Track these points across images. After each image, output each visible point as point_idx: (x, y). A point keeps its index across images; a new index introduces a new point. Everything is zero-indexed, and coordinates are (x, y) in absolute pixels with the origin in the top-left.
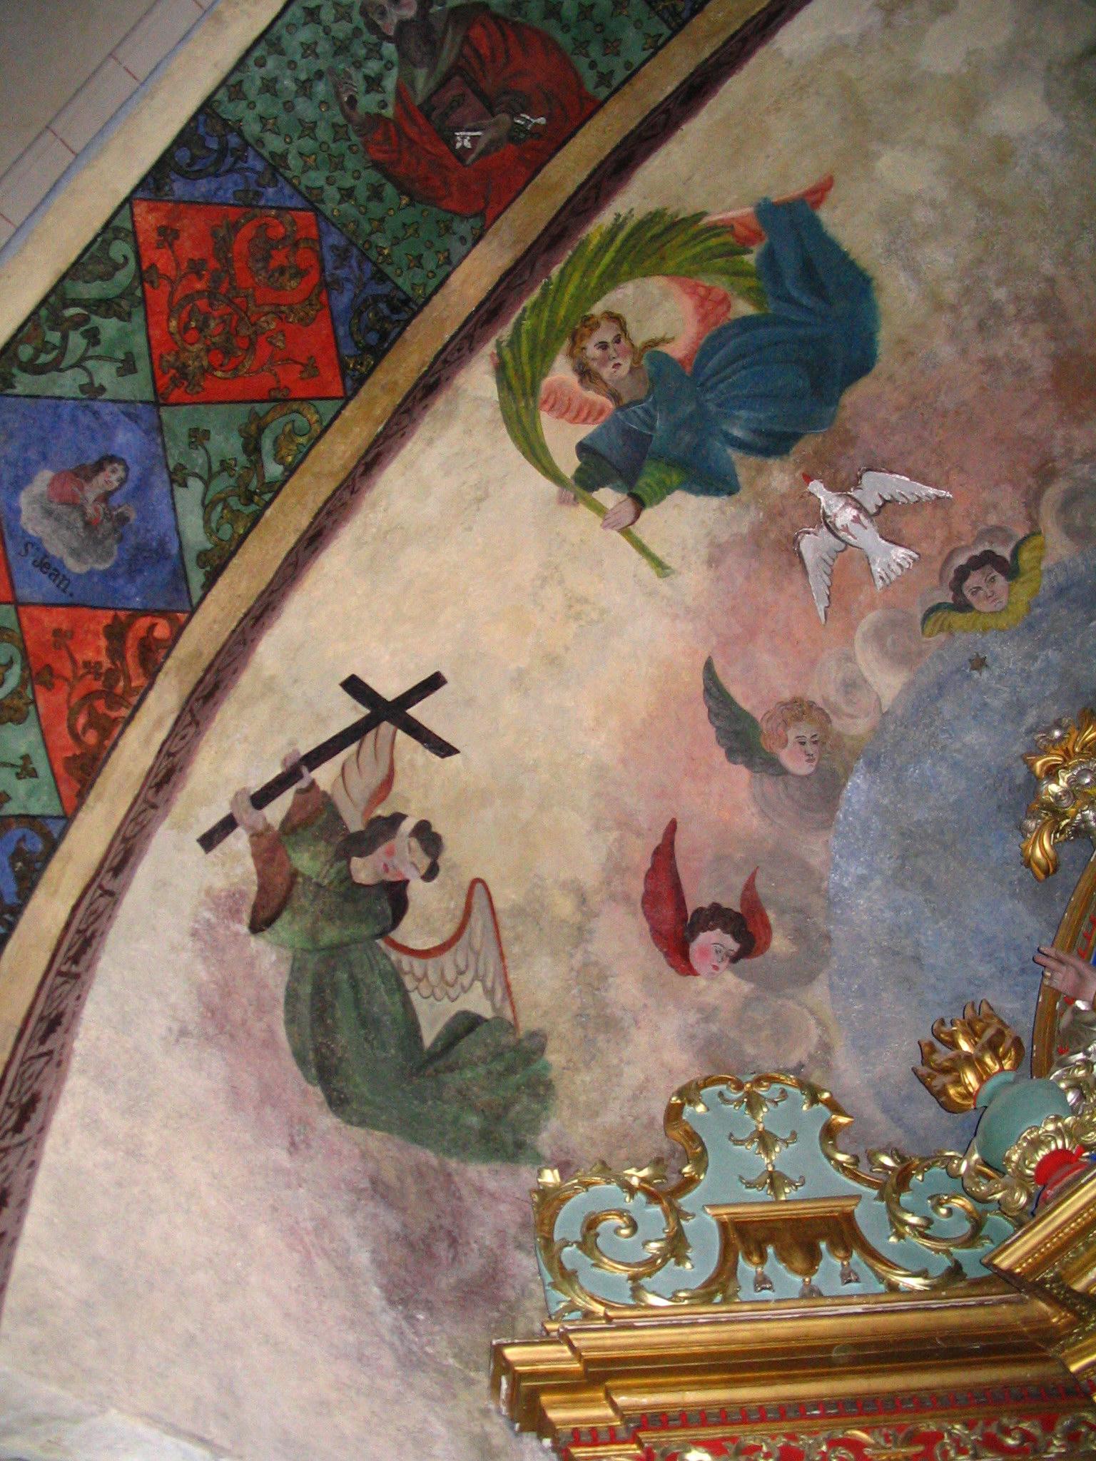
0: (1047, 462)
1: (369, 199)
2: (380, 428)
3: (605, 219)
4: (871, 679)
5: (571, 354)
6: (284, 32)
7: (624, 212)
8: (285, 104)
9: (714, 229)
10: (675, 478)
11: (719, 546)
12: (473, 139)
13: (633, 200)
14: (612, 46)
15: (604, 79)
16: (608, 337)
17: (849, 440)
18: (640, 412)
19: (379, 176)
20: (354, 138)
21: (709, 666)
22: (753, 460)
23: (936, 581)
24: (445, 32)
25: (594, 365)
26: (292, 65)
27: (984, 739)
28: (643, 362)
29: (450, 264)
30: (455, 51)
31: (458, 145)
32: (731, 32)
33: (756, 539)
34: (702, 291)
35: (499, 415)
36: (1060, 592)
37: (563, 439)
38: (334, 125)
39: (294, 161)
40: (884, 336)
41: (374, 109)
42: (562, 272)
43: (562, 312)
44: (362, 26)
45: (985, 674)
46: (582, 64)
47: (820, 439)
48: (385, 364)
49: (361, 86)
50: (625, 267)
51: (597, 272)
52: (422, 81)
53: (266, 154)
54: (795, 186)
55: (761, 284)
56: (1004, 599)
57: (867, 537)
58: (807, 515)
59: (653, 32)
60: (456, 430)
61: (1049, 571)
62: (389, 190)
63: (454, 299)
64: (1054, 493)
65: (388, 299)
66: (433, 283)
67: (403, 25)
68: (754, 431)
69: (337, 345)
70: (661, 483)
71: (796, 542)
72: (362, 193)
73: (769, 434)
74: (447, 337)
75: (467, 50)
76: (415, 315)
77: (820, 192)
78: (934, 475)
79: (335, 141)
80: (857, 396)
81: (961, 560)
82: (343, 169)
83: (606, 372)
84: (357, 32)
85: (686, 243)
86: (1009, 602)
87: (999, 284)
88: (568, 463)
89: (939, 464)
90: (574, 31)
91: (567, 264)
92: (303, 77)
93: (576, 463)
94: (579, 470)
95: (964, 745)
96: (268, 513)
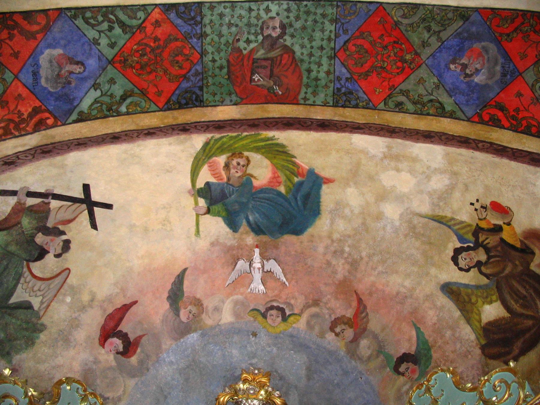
0: (319, 301)
1: (218, 67)
2: (162, 126)
3: (270, 134)
4: (223, 313)
5: (228, 158)
6: (239, 7)
7: (276, 137)
8: (221, 23)
9: (294, 164)
10: (224, 214)
11: (218, 242)
12: (259, 80)
13: (283, 137)
14: (315, 93)
15: (305, 99)
16: (242, 163)
17: (276, 247)
18: (231, 189)
19: (226, 65)
20: (230, 49)
21: (185, 270)
22: (248, 229)
23: (264, 303)
24: (278, 48)
25: (231, 166)
26: (233, 16)
27: (238, 355)
28: (244, 178)
29: (222, 103)
30: (276, 55)
31: (254, 77)
32: (347, 120)
33: (230, 249)
34: (276, 175)
35: (195, 155)
36: (292, 336)
37: (205, 176)
38: (228, 41)
39: (208, 39)
40: (310, 231)
41: (242, 47)
42: (247, 136)
43: (236, 146)
44: (260, 26)
45: (253, 339)
46: (304, 90)
47: (270, 240)
48: (180, 111)
49: (245, 39)
50: (263, 150)
51: (255, 145)
52: (260, 54)
53: (203, 30)
54: (325, 173)
55: (292, 188)
56: (276, 324)
57: (257, 276)
58: (248, 255)
59: (328, 101)
60: (181, 147)
61: (294, 328)
62: (225, 70)
63: (214, 113)
64: (314, 310)
65: (197, 96)
66: (214, 104)
67: (269, 36)
68: (255, 221)
69: (172, 95)
70: (219, 212)
71: (238, 259)
72: (217, 64)
73: (258, 226)
74: (203, 120)
75: (279, 58)
76: (200, 106)
77: (328, 181)
78: (289, 276)
79: (224, 45)
80: (289, 238)
81: (275, 304)
82: (219, 54)
83: (233, 171)
84: (257, 25)
85: (284, 160)
86: (277, 326)
87: (349, 246)
88: (200, 184)
89: (293, 275)
90: (309, 81)
91: (249, 135)
92: (232, 22)
93: (202, 186)
94: (201, 188)
95: (231, 352)
96: (111, 118)
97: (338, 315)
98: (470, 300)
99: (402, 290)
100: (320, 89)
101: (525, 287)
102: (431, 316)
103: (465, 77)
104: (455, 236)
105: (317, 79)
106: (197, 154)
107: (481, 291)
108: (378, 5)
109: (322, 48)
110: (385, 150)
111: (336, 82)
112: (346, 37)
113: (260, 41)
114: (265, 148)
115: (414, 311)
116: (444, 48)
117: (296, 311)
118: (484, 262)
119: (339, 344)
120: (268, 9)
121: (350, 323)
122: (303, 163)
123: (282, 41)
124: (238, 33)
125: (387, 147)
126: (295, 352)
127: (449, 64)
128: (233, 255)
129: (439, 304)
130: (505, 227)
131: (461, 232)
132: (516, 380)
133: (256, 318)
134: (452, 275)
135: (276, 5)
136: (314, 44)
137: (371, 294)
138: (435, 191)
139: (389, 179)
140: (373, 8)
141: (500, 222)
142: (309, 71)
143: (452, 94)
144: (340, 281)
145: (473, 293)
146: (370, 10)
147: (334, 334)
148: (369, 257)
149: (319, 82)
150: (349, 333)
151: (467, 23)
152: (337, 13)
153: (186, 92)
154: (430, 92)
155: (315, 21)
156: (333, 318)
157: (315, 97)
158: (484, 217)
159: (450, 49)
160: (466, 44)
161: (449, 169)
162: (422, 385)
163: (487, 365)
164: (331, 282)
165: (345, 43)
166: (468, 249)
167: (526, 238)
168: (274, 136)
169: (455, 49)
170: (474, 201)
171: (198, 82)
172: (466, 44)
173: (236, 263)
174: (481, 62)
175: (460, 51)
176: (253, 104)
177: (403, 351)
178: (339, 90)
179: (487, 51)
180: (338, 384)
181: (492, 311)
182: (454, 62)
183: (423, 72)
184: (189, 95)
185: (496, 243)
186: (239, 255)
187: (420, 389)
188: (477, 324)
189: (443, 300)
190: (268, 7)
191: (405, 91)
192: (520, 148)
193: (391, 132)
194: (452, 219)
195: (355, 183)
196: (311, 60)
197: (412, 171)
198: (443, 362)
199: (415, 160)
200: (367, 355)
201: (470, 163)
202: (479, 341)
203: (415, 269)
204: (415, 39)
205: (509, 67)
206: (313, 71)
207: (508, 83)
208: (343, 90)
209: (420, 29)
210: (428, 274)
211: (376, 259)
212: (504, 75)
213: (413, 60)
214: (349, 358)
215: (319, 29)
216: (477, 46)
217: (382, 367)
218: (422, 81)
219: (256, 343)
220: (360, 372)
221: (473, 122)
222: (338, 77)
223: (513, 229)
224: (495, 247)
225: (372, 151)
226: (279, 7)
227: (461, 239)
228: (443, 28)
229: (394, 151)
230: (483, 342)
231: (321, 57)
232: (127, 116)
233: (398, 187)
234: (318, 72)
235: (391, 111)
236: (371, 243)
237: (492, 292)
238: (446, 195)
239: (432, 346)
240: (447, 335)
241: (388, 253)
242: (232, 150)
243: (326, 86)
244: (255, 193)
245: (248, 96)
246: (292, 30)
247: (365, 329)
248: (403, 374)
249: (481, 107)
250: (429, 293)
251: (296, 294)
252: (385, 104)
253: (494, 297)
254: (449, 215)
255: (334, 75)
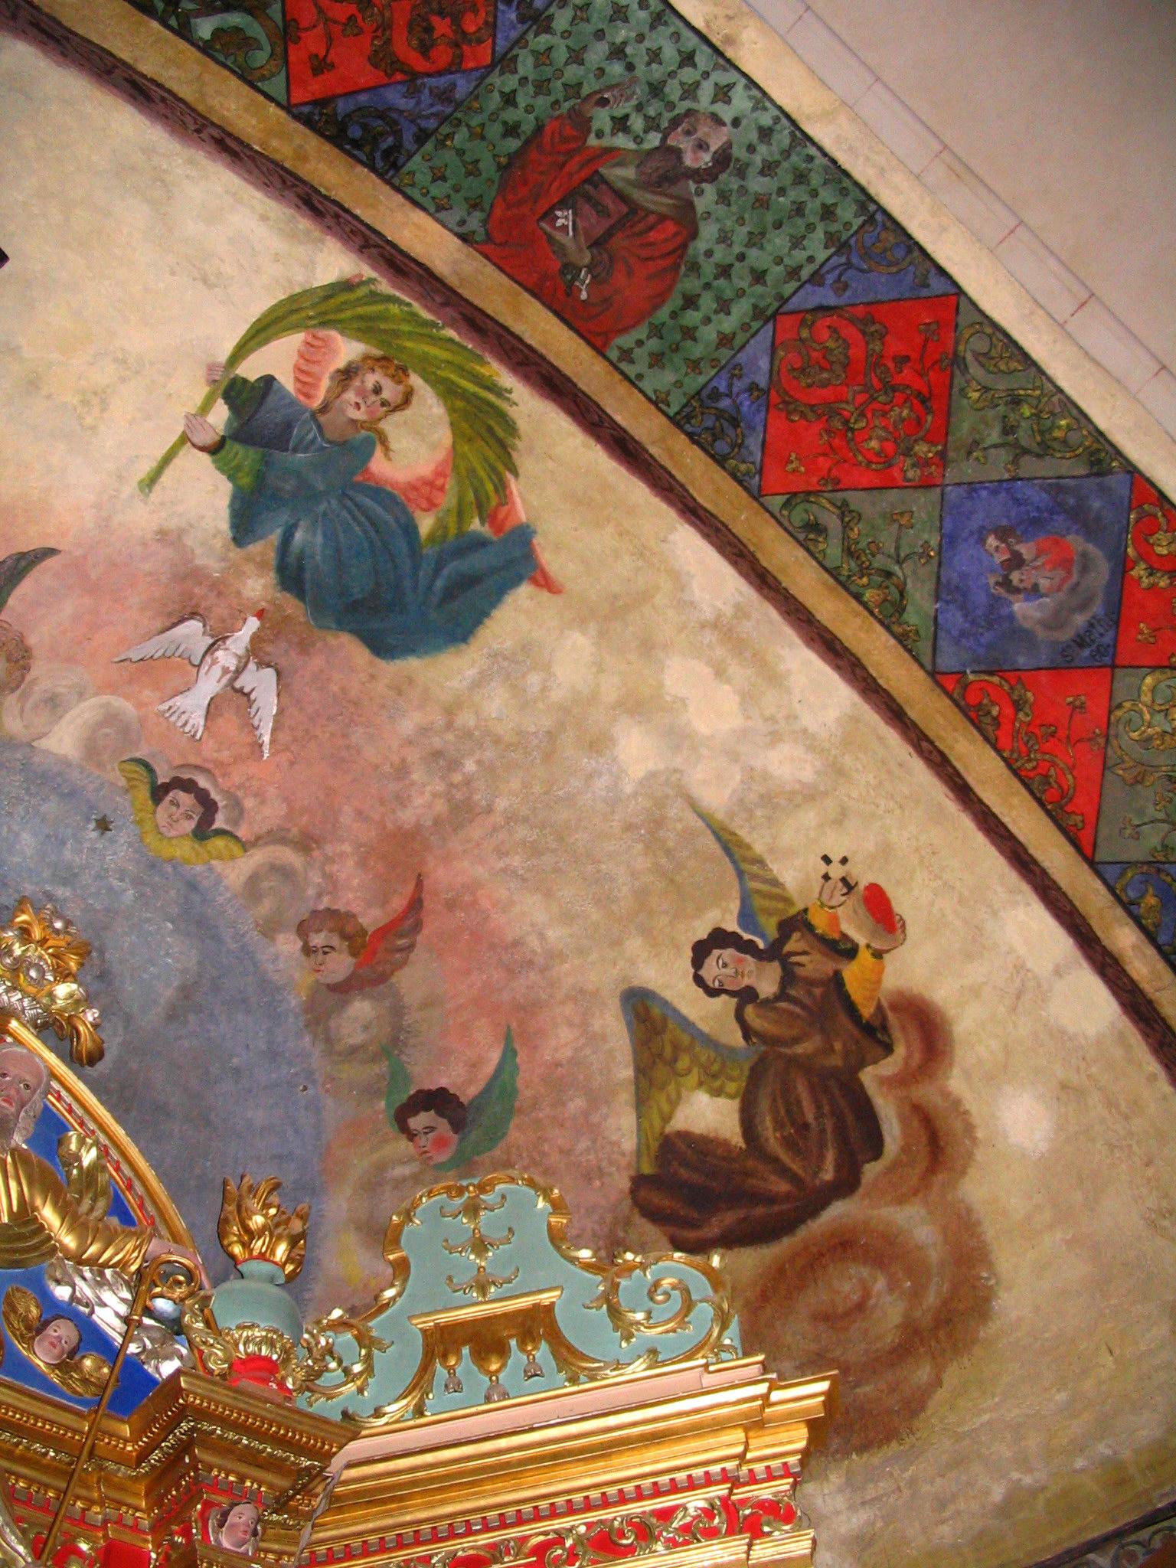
0: (317, 842)
1: (505, 123)
2: (257, 148)
3: (507, 379)
4: (63, 722)
5: (366, 357)
6: (672, 29)
7: (514, 396)
8: (602, 30)
9: (502, 487)
10: (245, 481)
11: (179, 537)
12: (564, 228)
13: (527, 406)
14: (657, 360)
15: (627, 355)
16: (386, 394)
17: (304, 647)
18: (310, 436)
19: (529, 133)
20: (566, 105)
21: (51, 552)
22: (272, 556)
23: (179, 761)
24: (671, 197)
25: (357, 383)
26: (641, 38)
27: (29, 852)
28: (363, 432)
29: (437, 209)
30: (652, 207)
31: (559, 213)
32: (674, 472)
33: (196, 575)
34: (439, 482)
35: (298, 290)
36: (193, 886)
37: (277, 360)
38: (580, 85)
39: (544, 39)
40: (412, 664)
41: (595, 125)
42: (451, 340)
43: (409, 344)
44: (676, 112)
45: (94, 835)
46: (641, 332)
47: (302, 619)
48: (327, 147)
49: (619, 112)
50: (460, 404)
51: (453, 377)
52: (622, 174)
53: (552, 10)
54: (549, 558)
55: (451, 537)
56: (173, 833)
57: (209, 685)
58: (223, 621)
59: (670, 399)
60: (277, 244)
61: (211, 869)
62: (513, 144)
63: (399, 217)
64: (289, 856)
65: (397, 147)
66: (417, 196)
67: (677, 153)
68: (302, 552)
69: (346, 94)
70: (239, 468)
71: (193, 615)
72: (510, 115)
73: (301, 568)
74: (358, 212)
75: (652, 219)
76: (381, 176)
77: (546, 583)
78: (284, 737)
79: (565, 85)
80: (352, 650)
81: (203, 782)
82: (536, 94)
83: (350, 396)
84: (671, 106)
85: (486, 460)
86: (171, 839)
87: (479, 762)
88: (251, 369)
89: (295, 740)
90: (670, 323)
91: (458, 344)
92: (629, 50)
93: (252, 377)
94: (245, 381)
95: (17, 835)
96: (155, 25)
97: (340, 906)
98: (675, 1060)
99: (533, 942)
100: (677, 359)
101: (819, 1107)
102: (561, 1041)
103: (997, 583)
104: (738, 903)
105: (689, 333)
106: (305, 293)
107: (713, 1054)
108: (953, 290)
109: (759, 277)
110: (729, 611)
111: (725, 374)
112: (832, 300)
113: (646, 146)
114: (468, 402)
115: (529, 1008)
116: (1007, 490)
117: (242, 832)
118: (762, 996)
119: (297, 975)
120: (726, 94)
121: (356, 940)
122: (523, 500)
123: (692, 186)
124: (617, 85)
125: (738, 607)
126: (176, 930)
127: (990, 531)
128: (189, 599)
129: (597, 1025)
130: (864, 955)
131: (758, 902)
132: (716, 1299)
133: (133, 787)
134: (671, 980)
135: (750, 97)
136: (753, 253)
137: (451, 905)
138: (766, 776)
139: (682, 676)
140: (937, 286)
141: (860, 939)
142: (690, 302)
143: (944, 596)
144: (400, 828)
145: (689, 1049)
146: (928, 286)
147: (300, 944)
148: (508, 820)
149: (689, 343)
150: (341, 965)
151: (1093, 481)
152: (856, 232)
153: (381, 116)
154: (902, 555)
155: (799, 210)
156: (325, 903)
157: (651, 366)
158: (833, 903)
159: (1018, 502)
160: (1060, 521)
161: (833, 752)
162: (461, 1191)
163: (628, 1223)
164: (377, 817)
165: (821, 308)
166: (748, 947)
167: (894, 1007)
168: (510, 392)
169: (1028, 512)
170: (836, 858)
171: (428, 117)
172: (1060, 521)
173: (182, 621)
174: (1057, 580)
175: (1033, 524)
176: (501, 269)
177: (444, 1082)
178: (716, 395)
179: (1085, 570)
180: (237, 1071)
181: (708, 1113)
182: (1003, 534)
183: (923, 504)
184: (378, 125)
185: (817, 975)
186: (203, 605)
187: (451, 1197)
188: (657, 1123)
189: (613, 1026)
190: (730, 86)
191: (851, 511)
192: (996, 810)
193: (763, 580)
194: (760, 861)
195: (602, 634)
196: (716, 283)
197: (748, 699)
198: (526, 1162)
199: (774, 678)
200: (351, 1041)
201: (889, 772)
202: (638, 1162)
203: (595, 915)
204: (963, 426)
205: (1102, 635)
206: (697, 309)
207: (1076, 663)
208: (725, 403)
209: (990, 414)
210: (617, 943)
211: (522, 832)
212: (1080, 642)
213: (922, 463)
214: (301, 1024)
215: (791, 231)
216: (1076, 542)
217: (371, 1092)
218: (904, 521)
219: (93, 850)
220: (310, 1074)
221: (938, 683)
222: (738, 366)
223: (881, 971)
224: (811, 983)
225: (696, 591)
226: (755, 109)
227: (746, 917)
228: (1036, 449)
229: (746, 627)
230: (647, 1169)
231: (741, 293)
232: (198, 54)
233: (691, 709)
234: (707, 320)
235: (786, 529)
236: (537, 789)
237: (736, 1073)
238: (783, 802)
239: (519, 1110)
240: (572, 1106)
241: (560, 839)
242: (390, 345)
243: (695, 365)
244: (356, 486)
245: (505, 241)
246: (735, 184)
247: (383, 978)
248: (411, 1136)
249: (983, 667)
250: (590, 987)
251: (272, 791)
252: (786, 505)
253: (732, 1087)
254: (759, 848)
255: (734, 356)
